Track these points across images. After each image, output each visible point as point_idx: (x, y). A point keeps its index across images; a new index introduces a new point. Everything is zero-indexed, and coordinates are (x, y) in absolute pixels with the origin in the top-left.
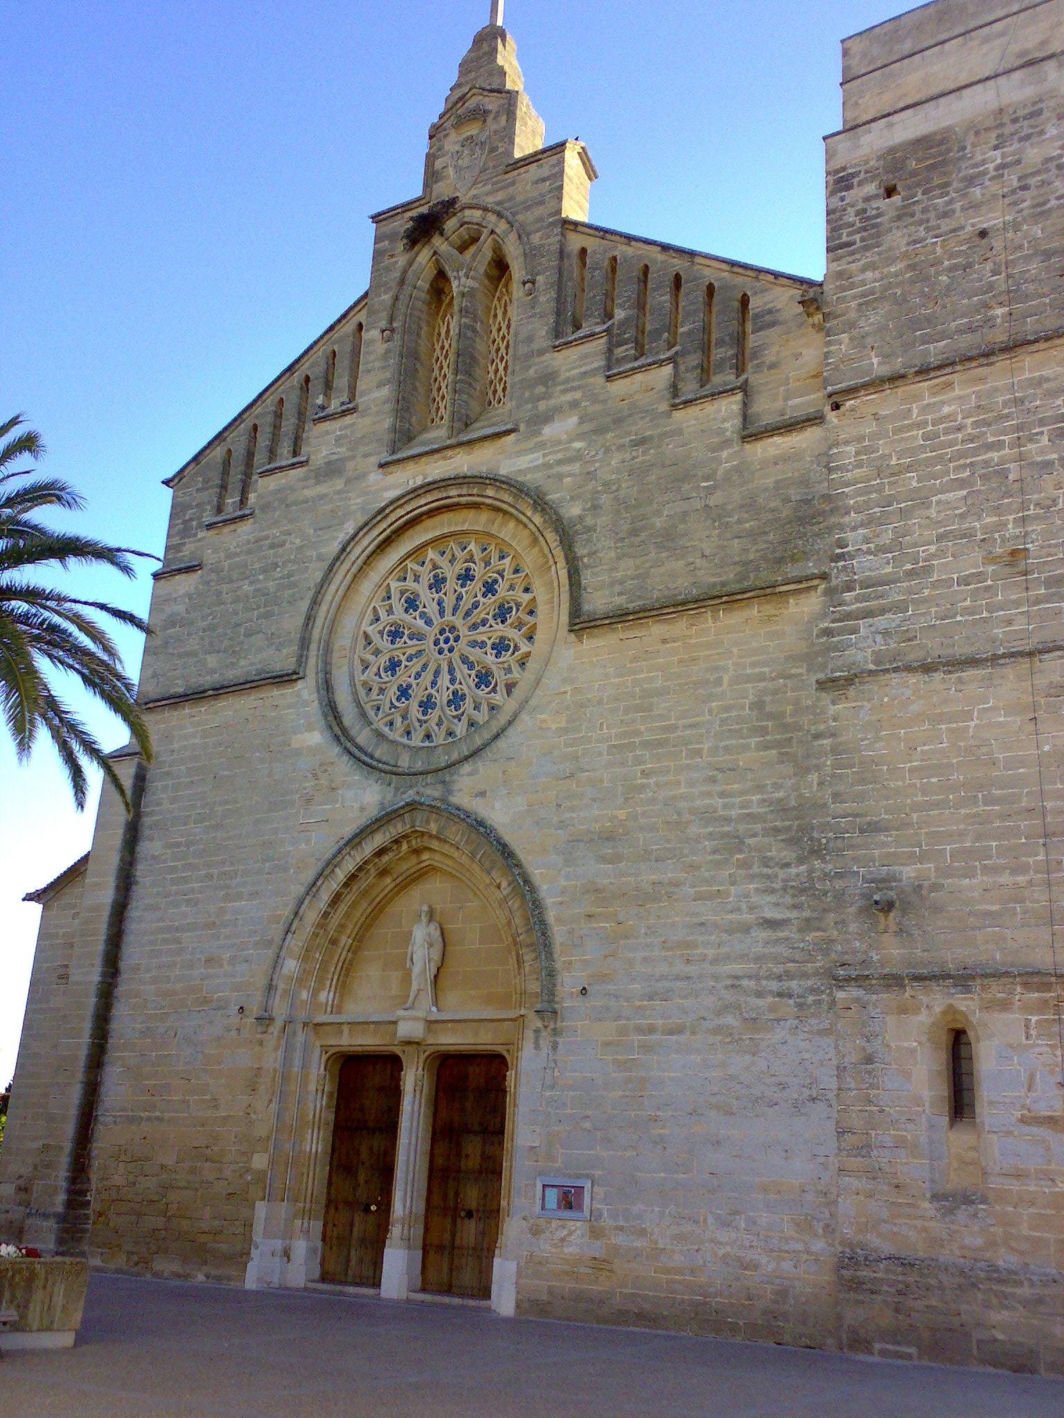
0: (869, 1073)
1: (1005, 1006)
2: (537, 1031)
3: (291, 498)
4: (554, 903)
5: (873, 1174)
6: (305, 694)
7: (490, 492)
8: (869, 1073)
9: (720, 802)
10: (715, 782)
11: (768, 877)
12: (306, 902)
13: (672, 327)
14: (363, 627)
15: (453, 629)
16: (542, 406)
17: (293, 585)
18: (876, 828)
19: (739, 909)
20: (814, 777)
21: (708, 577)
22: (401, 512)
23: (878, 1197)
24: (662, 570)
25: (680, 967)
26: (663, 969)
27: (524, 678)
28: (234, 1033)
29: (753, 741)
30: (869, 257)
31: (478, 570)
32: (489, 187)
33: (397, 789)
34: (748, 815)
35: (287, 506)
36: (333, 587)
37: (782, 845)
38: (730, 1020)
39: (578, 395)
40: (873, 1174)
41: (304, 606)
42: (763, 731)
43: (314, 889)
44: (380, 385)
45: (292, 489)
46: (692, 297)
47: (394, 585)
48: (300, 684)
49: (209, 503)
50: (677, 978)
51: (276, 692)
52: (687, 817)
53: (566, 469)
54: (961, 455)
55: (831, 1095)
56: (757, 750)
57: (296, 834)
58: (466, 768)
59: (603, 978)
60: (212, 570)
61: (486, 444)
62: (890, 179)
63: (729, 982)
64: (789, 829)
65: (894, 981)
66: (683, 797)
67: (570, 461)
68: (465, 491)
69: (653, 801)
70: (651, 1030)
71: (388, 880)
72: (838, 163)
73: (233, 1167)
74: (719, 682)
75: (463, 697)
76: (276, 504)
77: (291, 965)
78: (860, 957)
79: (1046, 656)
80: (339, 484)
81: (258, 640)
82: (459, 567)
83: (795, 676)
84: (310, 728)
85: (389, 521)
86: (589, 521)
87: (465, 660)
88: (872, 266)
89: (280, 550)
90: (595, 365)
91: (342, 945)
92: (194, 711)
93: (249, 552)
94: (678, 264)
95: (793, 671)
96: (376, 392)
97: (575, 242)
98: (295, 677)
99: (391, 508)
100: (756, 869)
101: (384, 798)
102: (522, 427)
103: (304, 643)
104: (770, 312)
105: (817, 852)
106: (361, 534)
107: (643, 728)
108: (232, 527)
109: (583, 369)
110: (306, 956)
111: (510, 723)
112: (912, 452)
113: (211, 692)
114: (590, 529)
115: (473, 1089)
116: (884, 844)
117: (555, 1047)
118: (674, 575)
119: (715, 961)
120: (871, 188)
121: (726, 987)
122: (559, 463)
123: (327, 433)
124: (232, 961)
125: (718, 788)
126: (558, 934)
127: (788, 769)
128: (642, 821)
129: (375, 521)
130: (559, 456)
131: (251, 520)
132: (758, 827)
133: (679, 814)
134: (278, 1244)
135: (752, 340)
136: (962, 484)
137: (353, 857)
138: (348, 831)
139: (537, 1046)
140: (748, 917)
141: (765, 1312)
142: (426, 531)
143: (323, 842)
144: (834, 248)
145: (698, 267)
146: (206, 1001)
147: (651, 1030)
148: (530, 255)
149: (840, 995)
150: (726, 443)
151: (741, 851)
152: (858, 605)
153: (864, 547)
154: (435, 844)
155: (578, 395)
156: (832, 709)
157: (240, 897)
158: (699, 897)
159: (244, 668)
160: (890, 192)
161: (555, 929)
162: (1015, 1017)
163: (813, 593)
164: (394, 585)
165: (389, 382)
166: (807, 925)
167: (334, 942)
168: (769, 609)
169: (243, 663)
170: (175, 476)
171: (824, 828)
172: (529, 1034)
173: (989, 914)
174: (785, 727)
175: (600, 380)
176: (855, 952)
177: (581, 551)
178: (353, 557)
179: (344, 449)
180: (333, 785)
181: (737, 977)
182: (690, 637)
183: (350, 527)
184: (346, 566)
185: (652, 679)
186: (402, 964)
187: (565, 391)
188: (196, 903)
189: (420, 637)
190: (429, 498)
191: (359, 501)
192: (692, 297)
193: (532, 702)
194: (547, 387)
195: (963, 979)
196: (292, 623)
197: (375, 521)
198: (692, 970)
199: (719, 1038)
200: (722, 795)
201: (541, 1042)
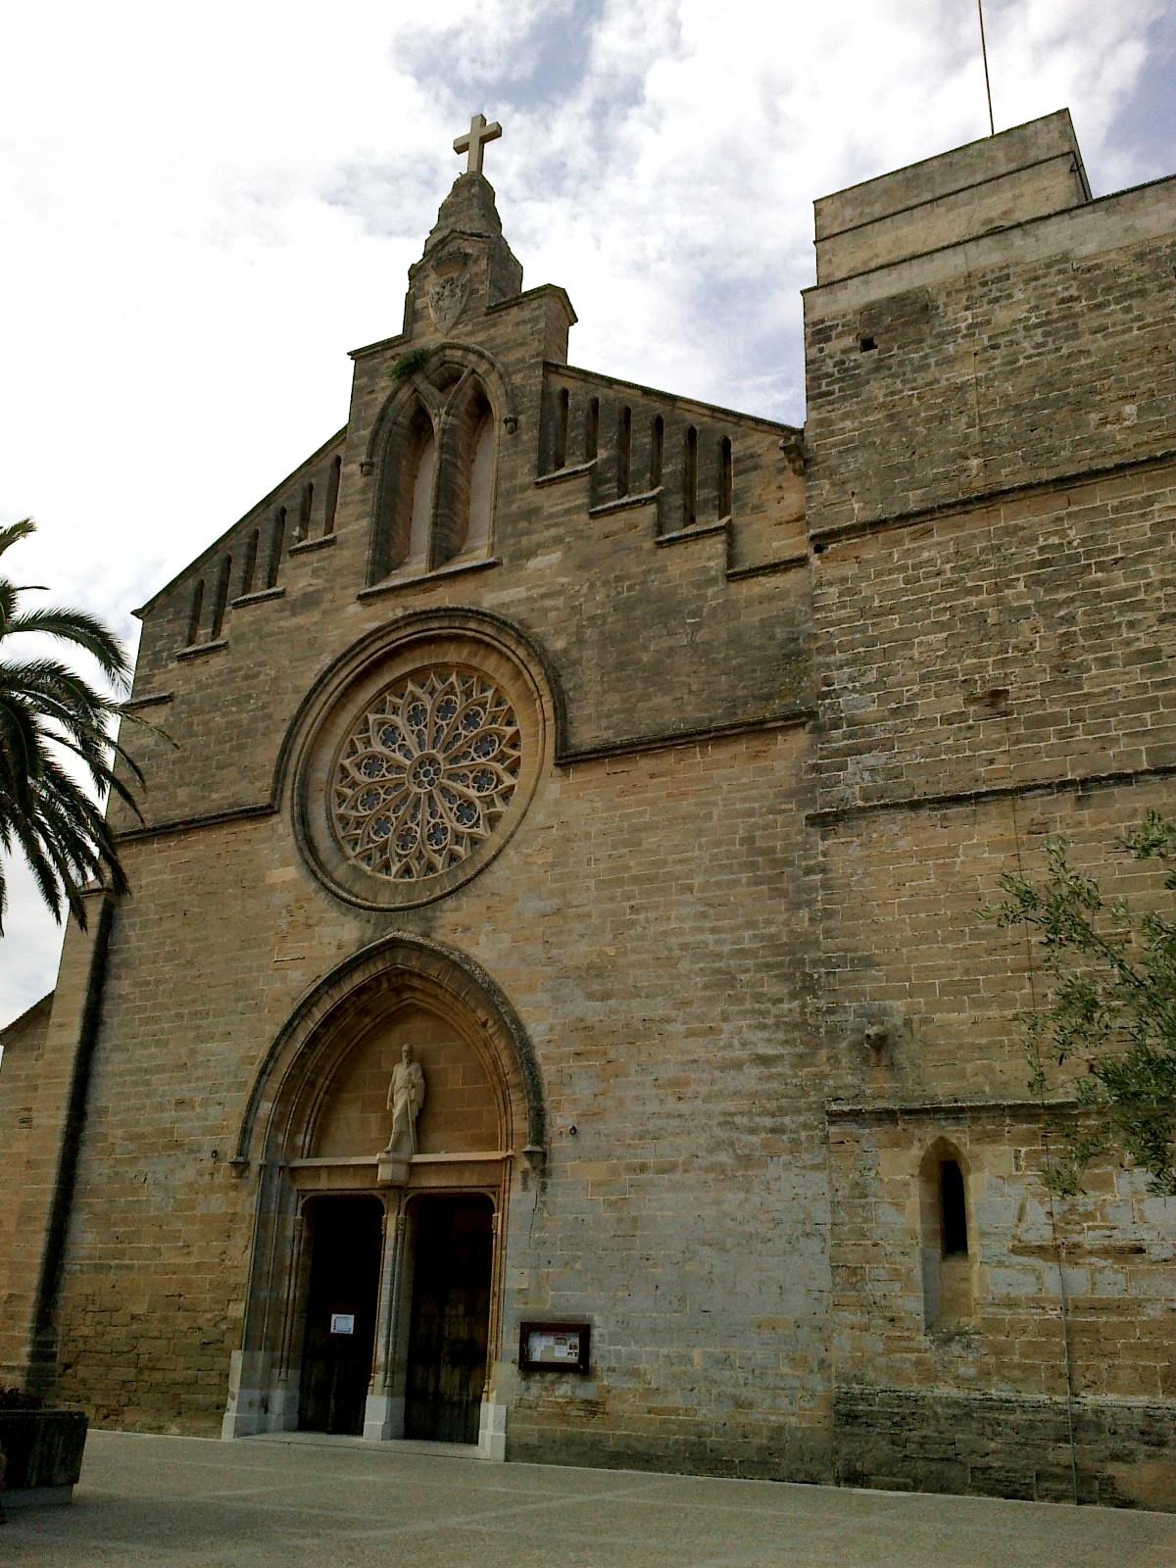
0: (863, 1207)
1: (994, 1138)
2: (525, 1173)
3: (266, 629)
4: (541, 1042)
5: (869, 1307)
6: (281, 829)
7: (472, 625)
8: (863, 1207)
9: (710, 938)
10: (706, 917)
11: (761, 1013)
12: (282, 1042)
13: (656, 470)
14: (340, 761)
15: (432, 761)
16: (524, 541)
17: (270, 717)
18: (869, 962)
19: (731, 1045)
20: (805, 913)
21: (694, 713)
22: (379, 644)
23: (872, 1330)
24: (650, 704)
25: (671, 1105)
26: (653, 1107)
27: (508, 811)
28: (207, 1177)
29: (744, 877)
30: (847, 407)
31: (459, 701)
32: (469, 327)
33: (376, 926)
34: (742, 949)
35: (261, 638)
36: (309, 720)
37: (774, 980)
38: (724, 1157)
39: (561, 530)
40: (869, 1307)
41: (279, 738)
42: (754, 866)
43: (290, 1030)
44: (359, 518)
46: (674, 441)
48: (275, 819)
49: (180, 633)
50: (669, 1116)
51: (249, 827)
52: (677, 953)
53: (549, 603)
54: (942, 598)
55: (826, 1230)
56: (748, 884)
57: (270, 972)
58: (450, 903)
59: (596, 1115)
60: (183, 702)
61: (469, 578)
62: (867, 332)
63: (721, 1119)
64: (780, 965)
65: (887, 1116)
66: (673, 932)
68: (446, 624)
69: (641, 938)
70: (643, 1168)
71: (367, 1020)
72: (816, 315)
73: (209, 1316)
74: (709, 817)
77: (266, 1107)
78: (852, 1092)
79: (1027, 794)
81: (230, 773)
82: (440, 698)
83: (784, 811)
86: (574, 654)
87: (444, 790)
88: (846, 416)
89: (255, 682)
91: (318, 1086)
92: (163, 845)
93: (222, 684)
94: (659, 407)
95: (783, 807)
96: (354, 524)
97: (558, 383)
98: (269, 811)
99: (371, 639)
100: (748, 1005)
101: (363, 935)
102: (505, 561)
103: (280, 775)
104: (752, 456)
105: (810, 987)
106: (339, 665)
107: (632, 864)
108: (204, 658)
109: (566, 506)
110: (283, 1097)
111: (495, 858)
112: (893, 594)
113: (181, 827)
114: (577, 662)
115: (456, 1239)
116: (876, 979)
117: (544, 1188)
118: (664, 711)
119: (707, 1099)
120: (849, 341)
121: (719, 1124)
122: (544, 596)
123: (304, 564)
124: (205, 1103)
125: (708, 924)
126: (548, 1073)
127: (781, 904)
128: (633, 957)
129: (354, 653)
130: (543, 590)
131: (225, 652)
132: (750, 963)
133: (670, 950)
134: (256, 1395)
135: (735, 483)
136: (942, 626)
137: (332, 997)
138: (326, 969)
139: (525, 1187)
140: (740, 1054)
141: (760, 1449)
143: (299, 981)
144: (814, 396)
145: (680, 411)
146: (178, 1145)
147: (643, 1168)
148: (512, 395)
149: (833, 1129)
150: (713, 581)
151: (733, 987)
152: (846, 742)
153: (850, 686)
154: (416, 983)
155: (561, 530)
156: (822, 846)
157: (211, 1037)
158: (691, 1034)
159: (220, 799)
160: (867, 345)
161: (544, 1068)
162: (1006, 1148)
163: (801, 729)
166: (801, 1060)
167: (311, 1084)
168: (757, 744)
169: (215, 796)
170: (144, 607)
171: (815, 963)
172: (517, 1176)
173: (980, 1047)
174: (775, 863)
175: (584, 517)
176: (846, 1087)
177: (567, 685)
178: (330, 688)
179: (320, 581)
181: (731, 1114)
182: (678, 772)
183: (327, 660)
184: (323, 698)
185: (640, 814)
186: (382, 1105)
187: (548, 527)
188: (166, 1044)
189: (400, 768)
190: (410, 630)
192: (674, 441)
193: (517, 837)
194: (530, 523)
195: (955, 1113)
196: (266, 754)
197: (354, 653)
198: (684, 1107)
199: (713, 1176)
200: (713, 930)
201: (530, 1183)
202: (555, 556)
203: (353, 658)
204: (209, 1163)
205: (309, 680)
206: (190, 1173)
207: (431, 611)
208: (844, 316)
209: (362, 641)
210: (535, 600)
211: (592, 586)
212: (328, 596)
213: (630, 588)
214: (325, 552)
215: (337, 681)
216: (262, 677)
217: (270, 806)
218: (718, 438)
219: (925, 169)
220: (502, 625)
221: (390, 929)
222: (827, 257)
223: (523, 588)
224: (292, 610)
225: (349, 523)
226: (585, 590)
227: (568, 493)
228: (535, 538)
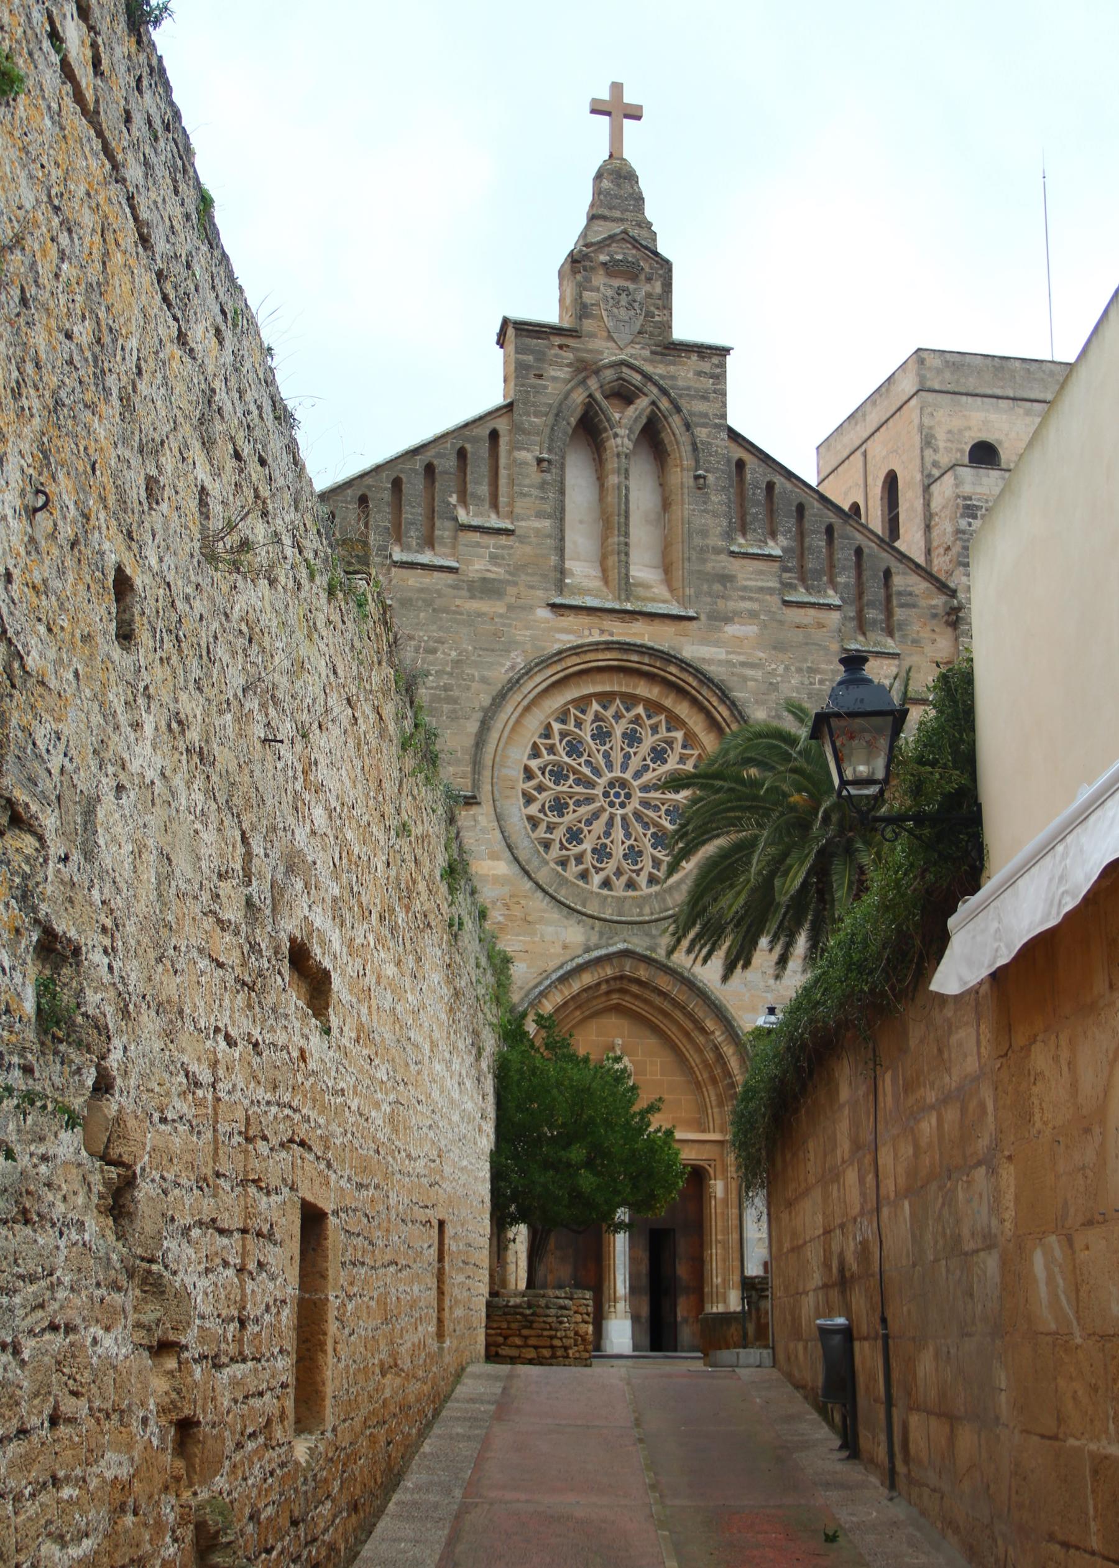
3: (438, 603)
7: (673, 669)
14: (525, 761)
16: (721, 603)
17: (455, 701)
33: (601, 934)
36: (503, 717)
39: (755, 606)
44: (540, 515)
45: (438, 591)
47: (556, 726)
48: (474, 810)
53: (749, 672)
61: (667, 621)
67: (752, 666)
68: (646, 660)
75: (640, 853)
76: (420, 603)
80: (500, 608)
84: (494, 856)
85: (563, 665)
89: (431, 657)
90: (770, 584)
101: (588, 940)
102: (703, 617)
104: (910, 594)
109: (760, 584)
122: (743, 664)
123: (478, 545)
130: (742, 658)
137: (561, 992)
142: (594, 683)
154: (634, 989)
155: (755, 606)
164: (556, 726)
165: (549, 517)
175: (774, 601)
180: (529, 918)
184: (518, 697)
187: (743, 598)
190: (609, 655)
191: (528, 633)
194: (725, 587)
202: (751, 630)
203: (548, 666)
205: (500, 674)
207: (635, 645)
208: (987, 501)
209: (560, 652)
210: (734, 665)
211: (787, 668)
212: (511, 590)
213: (821, 682)
214: (503, 540)
215: (531, 685)
216: (439, 654)
217: (474, 797)
218: (883, 567)
219: (1009, 364)
220: (706, 680)
221: (616, 939)
222: (930, 410)
223: (723, 650)
224: (469, 590)
225: (528, 518)
226: (781, 670)
227: (761, 572)
228: (731, 605)
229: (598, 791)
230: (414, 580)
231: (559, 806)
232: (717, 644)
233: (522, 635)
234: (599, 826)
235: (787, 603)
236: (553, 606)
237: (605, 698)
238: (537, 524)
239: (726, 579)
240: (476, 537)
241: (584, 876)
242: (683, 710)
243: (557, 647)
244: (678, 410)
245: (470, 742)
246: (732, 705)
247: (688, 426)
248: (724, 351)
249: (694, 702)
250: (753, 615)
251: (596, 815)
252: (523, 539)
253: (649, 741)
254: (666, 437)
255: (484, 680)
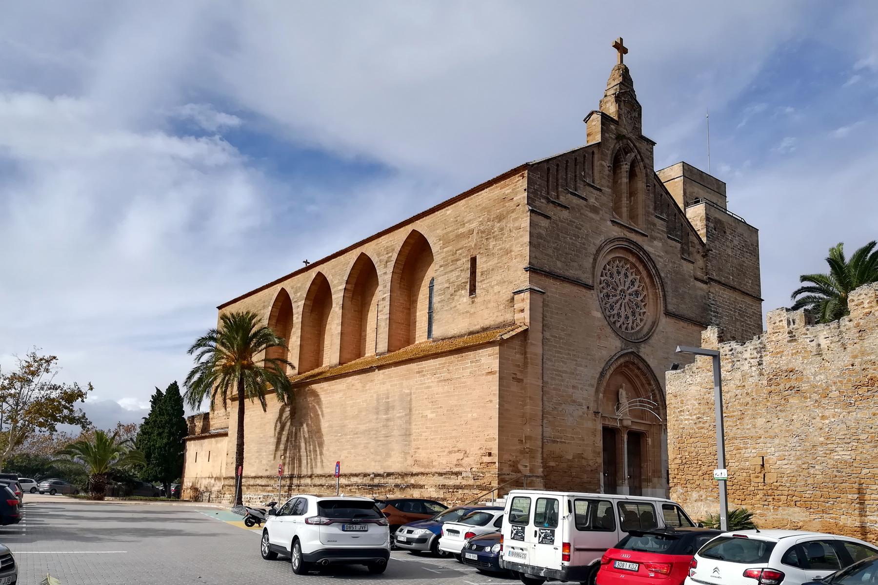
17: (586, 249)
48: (592, 292)
58: (643, 345)
146: (574, 401)
157: (581, 366)
204: (585, 410)
206: (581, 413)
214: (598, 193)
220: (650, 259)
229: (618, 292)
230: (575, 200)
231: (608, 296)
232: (652, 246)
233: (604, 229)
234: (618, 305)
235: (669, 237)
236: (612, 221)
237: (620, 259)
238: (607, 190)
239: (654, 225)
240: (592, 189)
241: (614, 323)
242: (641, 268)
243: (612, 237)
244: (643, 160)
245: (590, 266)
246: (657, 270)
247: (645, 167)
248: (654, 144)
249: (645, 266)
250: (661, 239)
251: (617, 301)
252: (604, 194)
253: (630, 278)
254: (637, 170)
255: (594, 244)
